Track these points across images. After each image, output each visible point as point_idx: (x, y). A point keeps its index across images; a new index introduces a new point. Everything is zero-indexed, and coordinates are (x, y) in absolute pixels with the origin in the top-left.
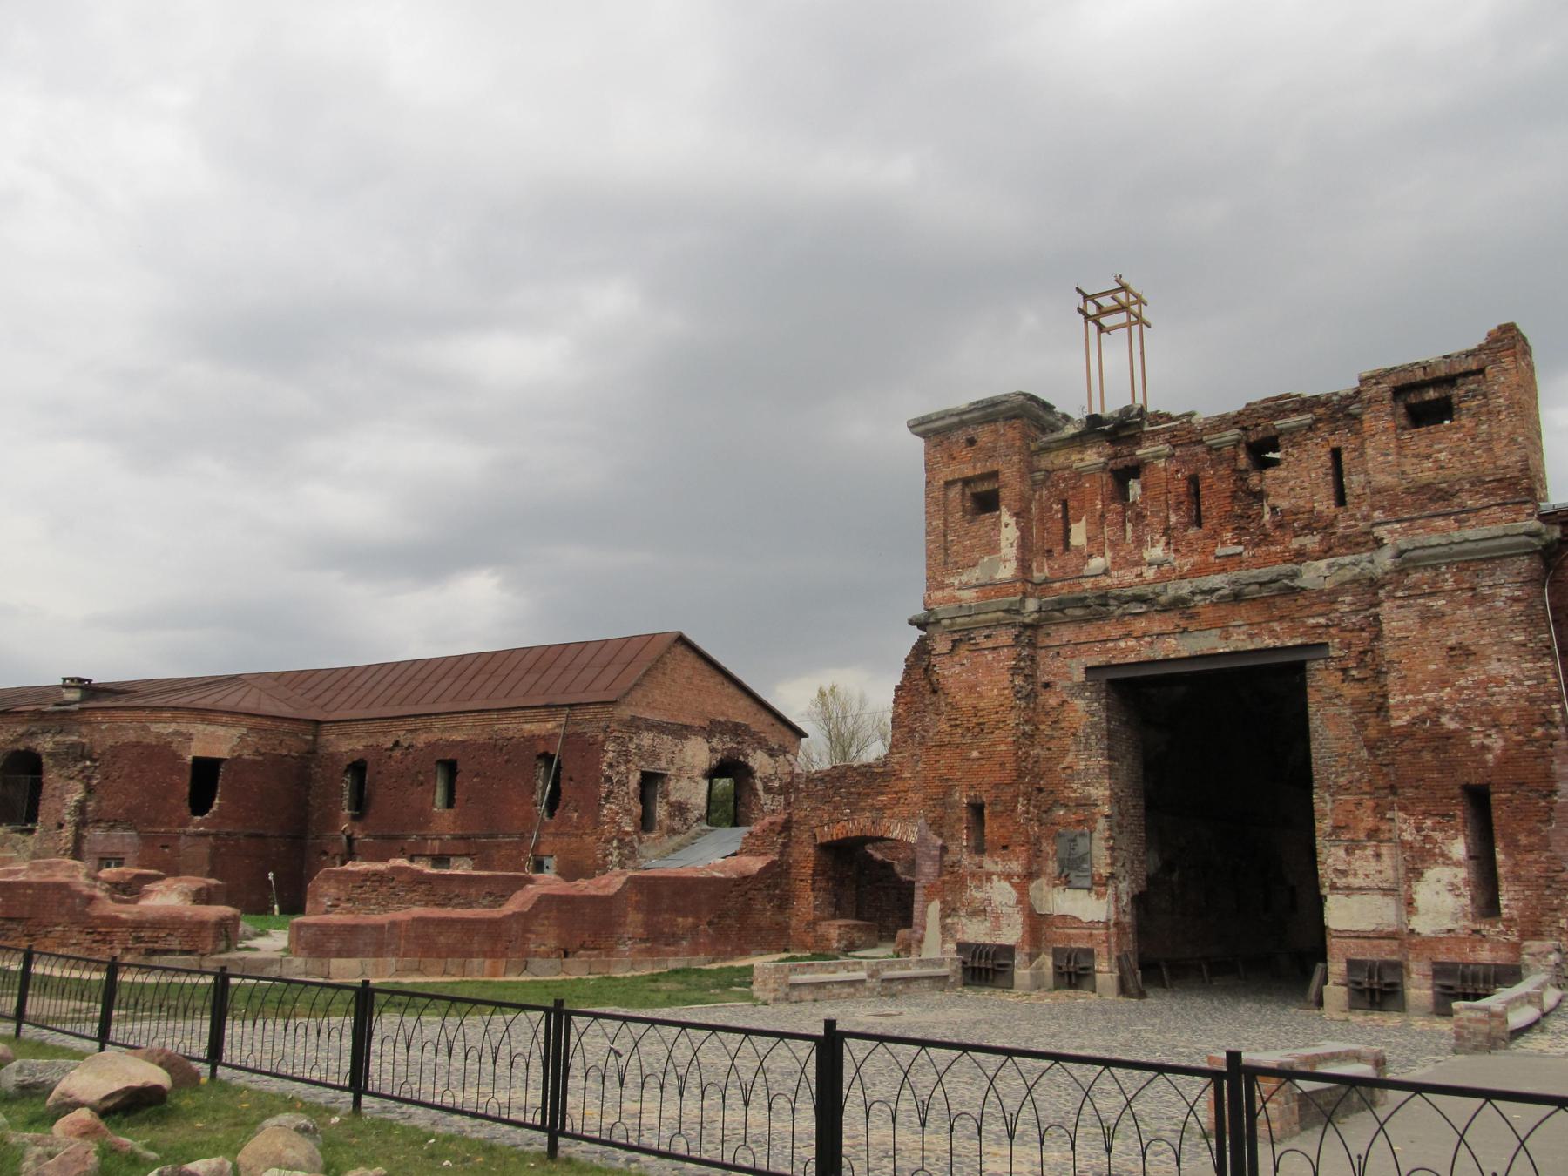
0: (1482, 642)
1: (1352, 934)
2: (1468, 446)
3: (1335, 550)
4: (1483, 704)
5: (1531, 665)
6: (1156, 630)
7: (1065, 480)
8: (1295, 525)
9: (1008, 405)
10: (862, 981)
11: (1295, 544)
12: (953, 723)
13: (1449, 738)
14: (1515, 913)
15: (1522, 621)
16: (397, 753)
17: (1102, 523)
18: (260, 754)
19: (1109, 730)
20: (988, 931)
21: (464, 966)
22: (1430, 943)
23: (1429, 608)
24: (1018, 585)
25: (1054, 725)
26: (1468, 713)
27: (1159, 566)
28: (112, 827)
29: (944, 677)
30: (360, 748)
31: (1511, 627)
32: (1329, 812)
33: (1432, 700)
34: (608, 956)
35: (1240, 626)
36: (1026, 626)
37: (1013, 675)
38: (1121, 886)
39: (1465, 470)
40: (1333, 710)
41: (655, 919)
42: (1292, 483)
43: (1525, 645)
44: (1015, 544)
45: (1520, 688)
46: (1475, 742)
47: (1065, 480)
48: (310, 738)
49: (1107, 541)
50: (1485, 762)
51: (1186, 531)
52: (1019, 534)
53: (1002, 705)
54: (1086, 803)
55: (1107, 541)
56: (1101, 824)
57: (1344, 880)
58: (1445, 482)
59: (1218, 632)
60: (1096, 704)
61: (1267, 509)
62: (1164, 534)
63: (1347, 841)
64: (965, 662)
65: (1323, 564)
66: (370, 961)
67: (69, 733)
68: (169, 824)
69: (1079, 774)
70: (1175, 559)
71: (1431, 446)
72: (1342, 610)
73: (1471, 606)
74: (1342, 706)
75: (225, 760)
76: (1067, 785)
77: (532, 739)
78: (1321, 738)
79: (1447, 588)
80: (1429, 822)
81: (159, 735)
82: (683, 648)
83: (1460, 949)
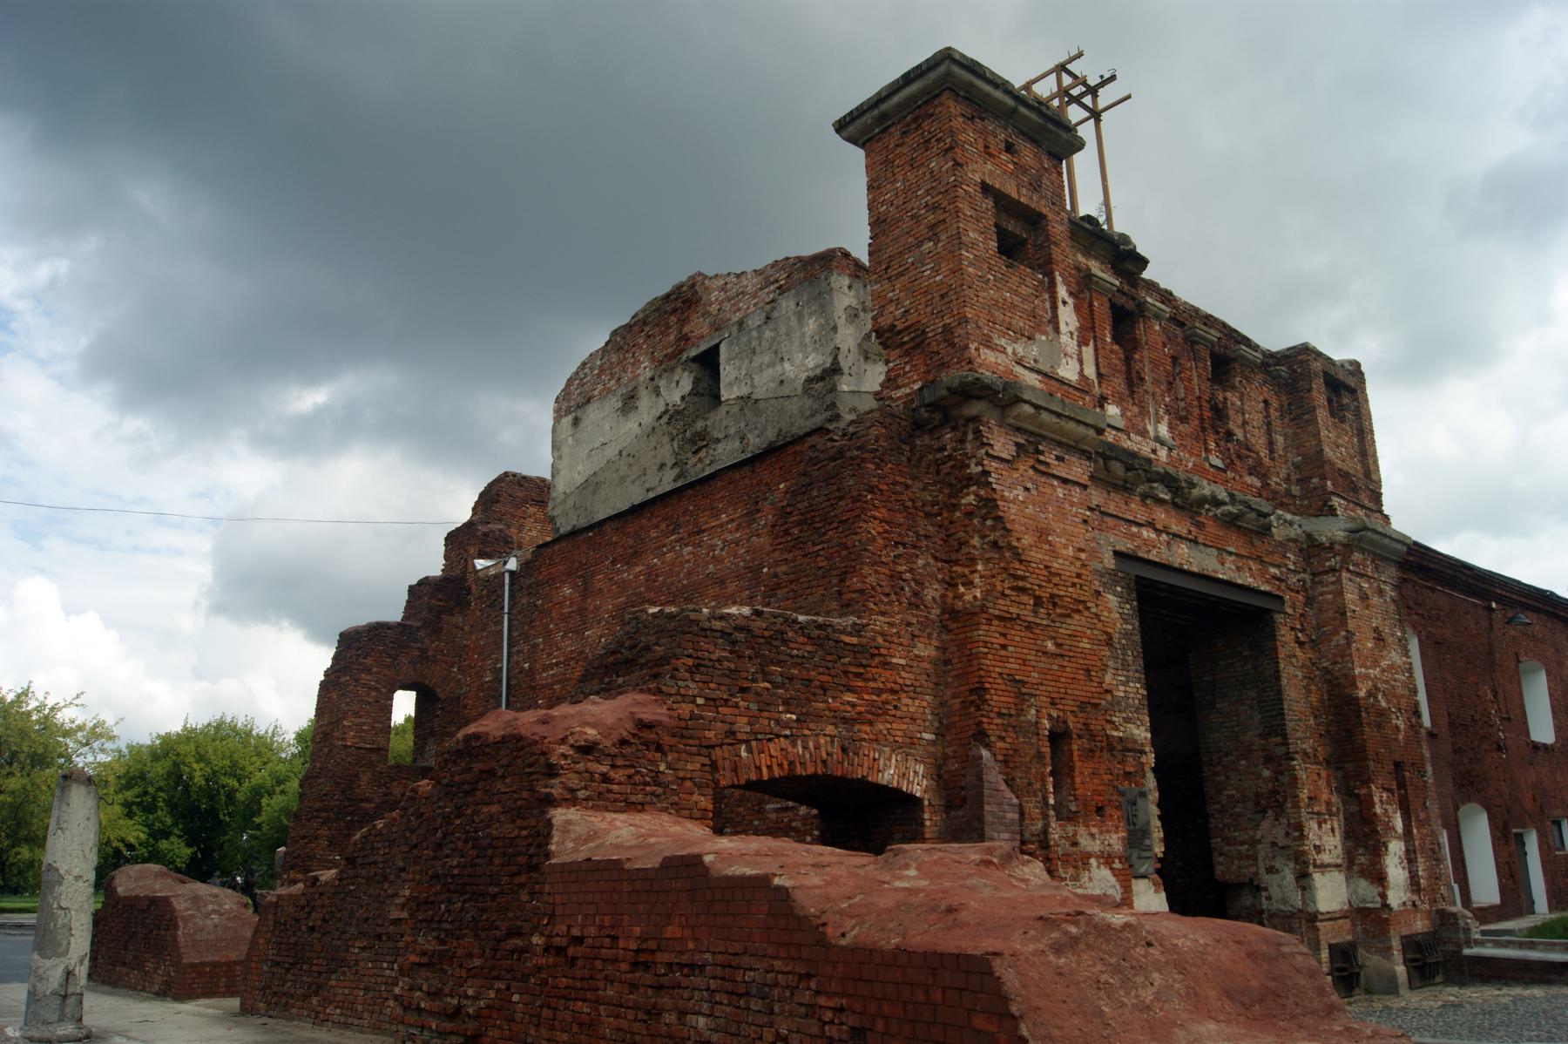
1: (1328, 916)
12: (1021, 584)
29: (1003, 498)
35: (1230, 553)
44: (1075, 337)
53: (1079, 576)
54: (1128, 747)
69: (1119, 703)
76: (1109, 718)
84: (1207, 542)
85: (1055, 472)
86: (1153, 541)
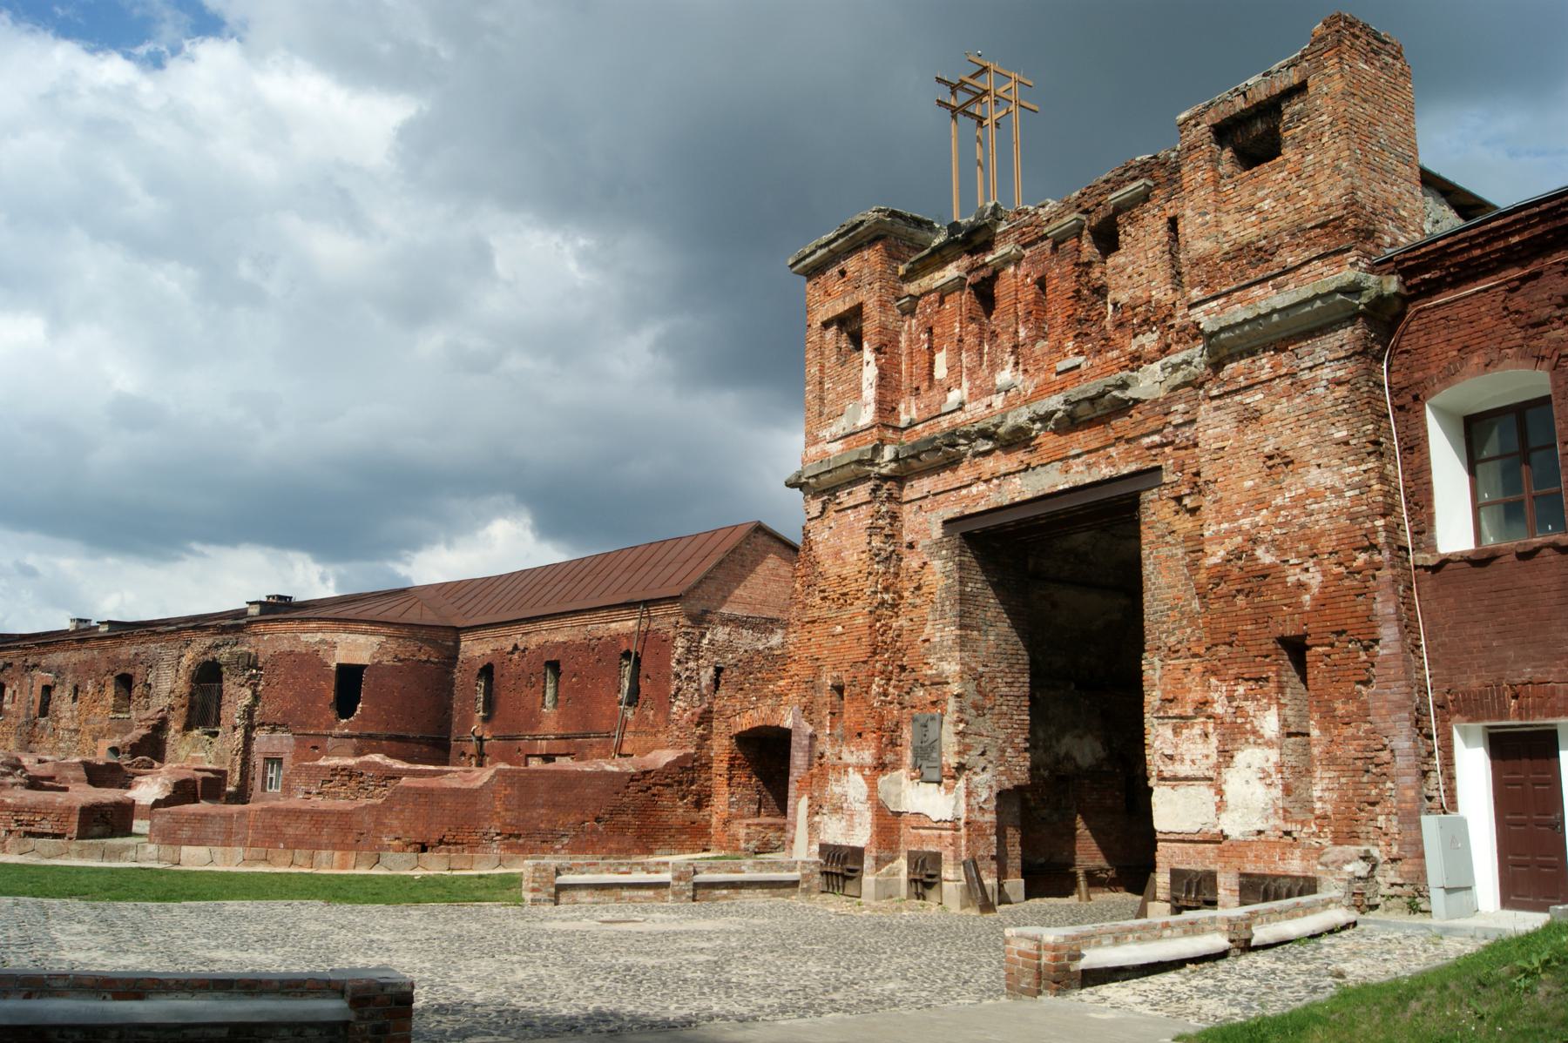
0: (1300, 444)
1: (1178, 837)
2: (1292, 187)
3: (1174, 347)
4: (1302, 527)
5: (1354, 469)
6: (1003, 469)
7: (931, 304)
8: (1135, 321)
9: (865, 225)
10: (665, 885)
11: (1133, 345)
13: (1265, 577)
14: (1329, 807)
15: (1345, 410)
16: (516, 656)
17: (960, 349)
18: (400, 660)
19: (962, 593)
20: (843, 831)
21: (312, 857)
22: (1241, 847)
23: (1246, 407)
24: (874, 430)
25: (917, 593)
26: (1284, 542)
27: (1007, 391)
28: (274, 730)
29: (817, 543)
30: (489, 652)
31: (1333, 420)
32: (1157, 682)
33: (1248, 527)
34: (471, 852)
35: (1078, 456)
36: (885, 478)
37: (870, 536)
38: (976, 779)
39: (1290, 218)
40: (1164, 551)
41: (528, 814)
42: (1129, 270)
43: (1347, 443)
45: (1341, 502)
46: (1291, 580)
47: (931, 304)
48: (451, 644)
49: (965, 370)
50: (1300, 605)
51: (1033, 346)
52: (877, 372)
54: (940, 682)
55: (965, 370)
56: (952, 705)
57: (1171, 767)
58: (1265, 238)
59: (1058, 465)
60: (951, 564)
61: (1110, 307)
62: (1012, 353)
63: (1174, 718)
64: (832, 525)
65: (1157, 366)
66: (218, 850)
67: (243, 644)
68: (318, 726)
70: (1023, 381)
71: (1254, 194)
72: (1174, 423)
73: (1290, 397)
74: (1174, 545)
75: (367, 666)
76: (925, 661)
77: (617, 638)
78: (1153, 587)
79: (1264, 377)
80: (1241, 689)
81: (307, 644)
82: (765, 538)
83: (1270, 857)
84: (1041, 462)
85: (846, 506)
86: (983, 491)
